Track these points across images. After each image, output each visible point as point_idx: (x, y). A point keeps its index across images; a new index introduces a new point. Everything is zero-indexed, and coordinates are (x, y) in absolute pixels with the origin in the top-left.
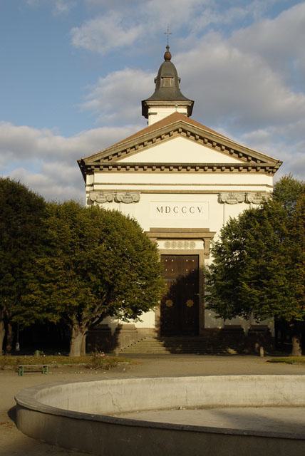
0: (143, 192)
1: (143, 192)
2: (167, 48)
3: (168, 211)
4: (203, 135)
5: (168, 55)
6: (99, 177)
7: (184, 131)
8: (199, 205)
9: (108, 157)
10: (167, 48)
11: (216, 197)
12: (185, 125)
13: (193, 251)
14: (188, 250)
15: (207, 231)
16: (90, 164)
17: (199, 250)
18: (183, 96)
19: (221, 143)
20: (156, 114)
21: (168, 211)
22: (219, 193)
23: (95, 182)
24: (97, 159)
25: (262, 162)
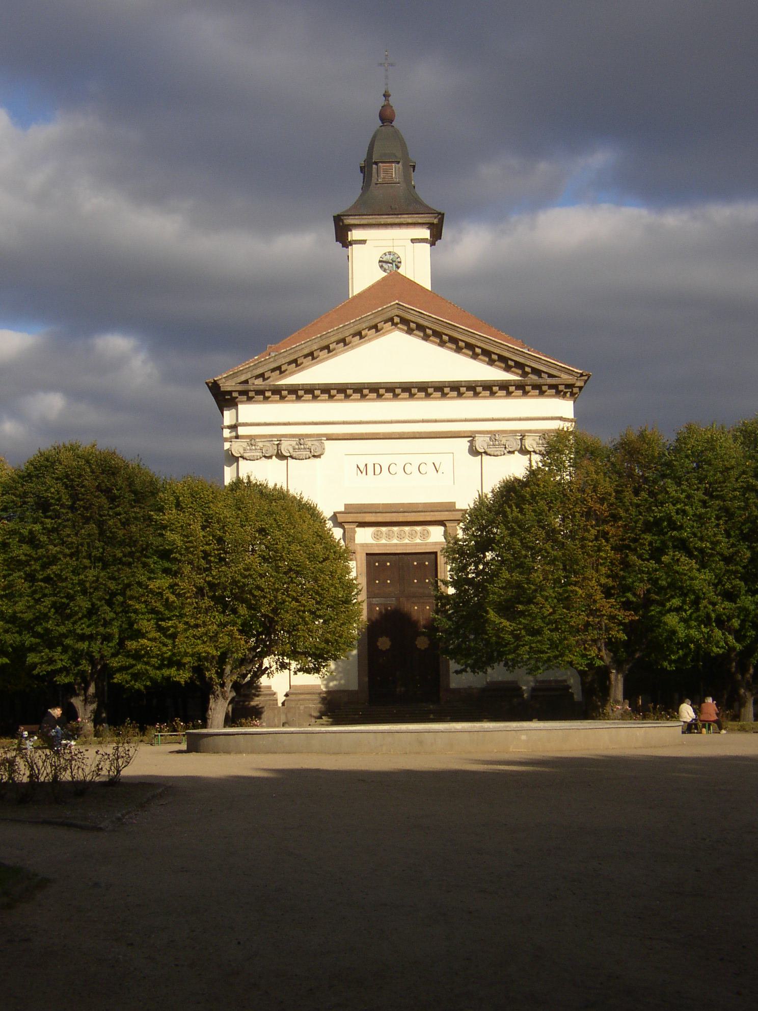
0: (330, 438)
1: (330, 438)
2: (386, 96)
4: (438, 329)
5: (388, 112)
6: (248, 412)
7: (404, 321)
8: (437, 459)
9: (262, 375)
10: (386, 96)
11: (464, 443)
12: (406, 309)
13: (426, 544)
14: (417, 544)
16: (229, 389)
17: (436, 543)
18: (421, 203)
19: (473, 341)
20: (363, 242)
22: (471, 436)
23: (240, 421)
24: (243, 378)
25: (551, 376)
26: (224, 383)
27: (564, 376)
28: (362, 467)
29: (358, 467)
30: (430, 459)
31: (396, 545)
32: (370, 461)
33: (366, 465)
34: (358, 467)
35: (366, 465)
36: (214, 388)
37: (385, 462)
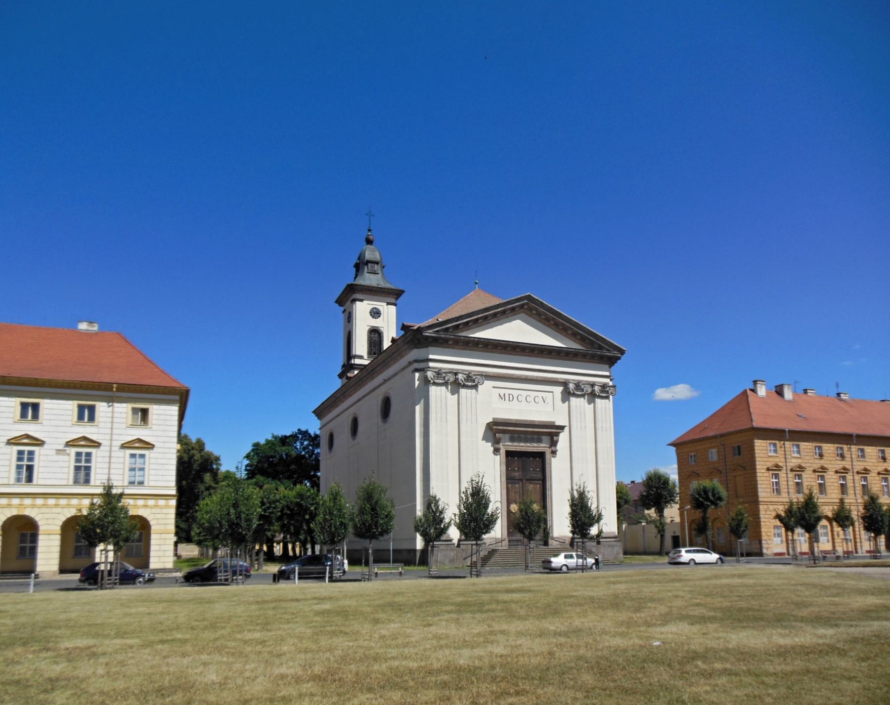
15: (552, 426)
22: (565, 384)
28: (502, 396)
29: (500, 395)
33: (504, 395)
34: (500, 395)
35: (504, 395)
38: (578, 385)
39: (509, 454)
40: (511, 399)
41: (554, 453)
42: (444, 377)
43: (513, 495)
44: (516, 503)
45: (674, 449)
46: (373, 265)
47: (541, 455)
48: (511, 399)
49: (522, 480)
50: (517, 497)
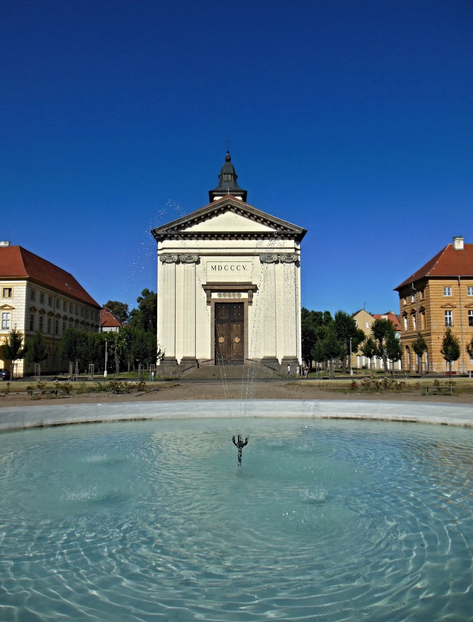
3: (220, 267)
9: (173, 229)
17: (243, 299)
21: (220, 267)
24: (166, 229)
25: (291, 230)
26: (158, 231)
27: (297, 230)
30: (241, 264)
31: (227, 299)
32: (217, 264)
36: (154, 232)
37: (223, 265)
38: (270, 255)
39: (216, 304)
40: (220, 269)
41: (251, 302)
42: (173, 258)
43: (220, 332)
44: (223, 336)
45: (397, 293)
46: (228, 175)
47: (242, 304)
48: (220, 269)
49: (227, 321)
50: (224, 332)
